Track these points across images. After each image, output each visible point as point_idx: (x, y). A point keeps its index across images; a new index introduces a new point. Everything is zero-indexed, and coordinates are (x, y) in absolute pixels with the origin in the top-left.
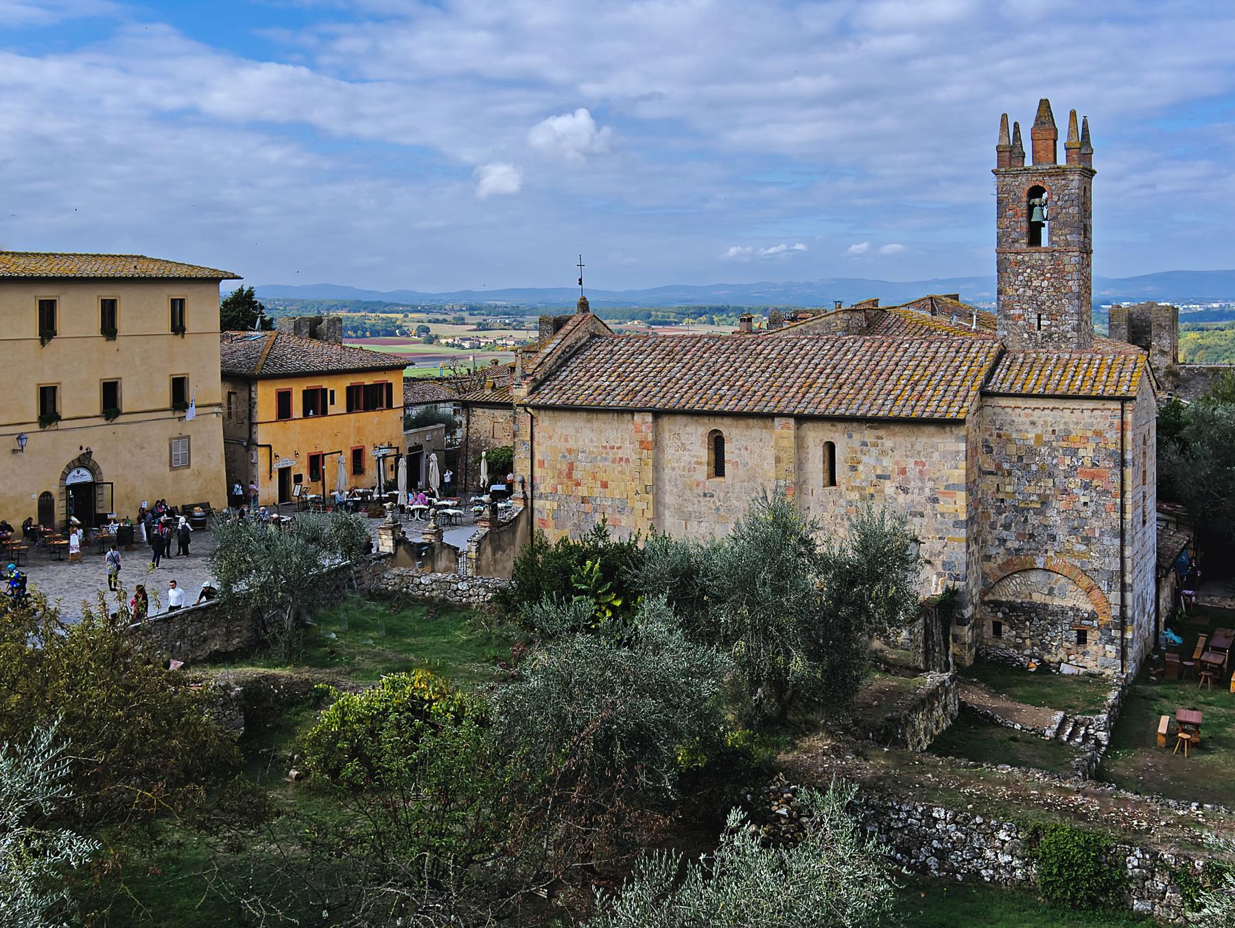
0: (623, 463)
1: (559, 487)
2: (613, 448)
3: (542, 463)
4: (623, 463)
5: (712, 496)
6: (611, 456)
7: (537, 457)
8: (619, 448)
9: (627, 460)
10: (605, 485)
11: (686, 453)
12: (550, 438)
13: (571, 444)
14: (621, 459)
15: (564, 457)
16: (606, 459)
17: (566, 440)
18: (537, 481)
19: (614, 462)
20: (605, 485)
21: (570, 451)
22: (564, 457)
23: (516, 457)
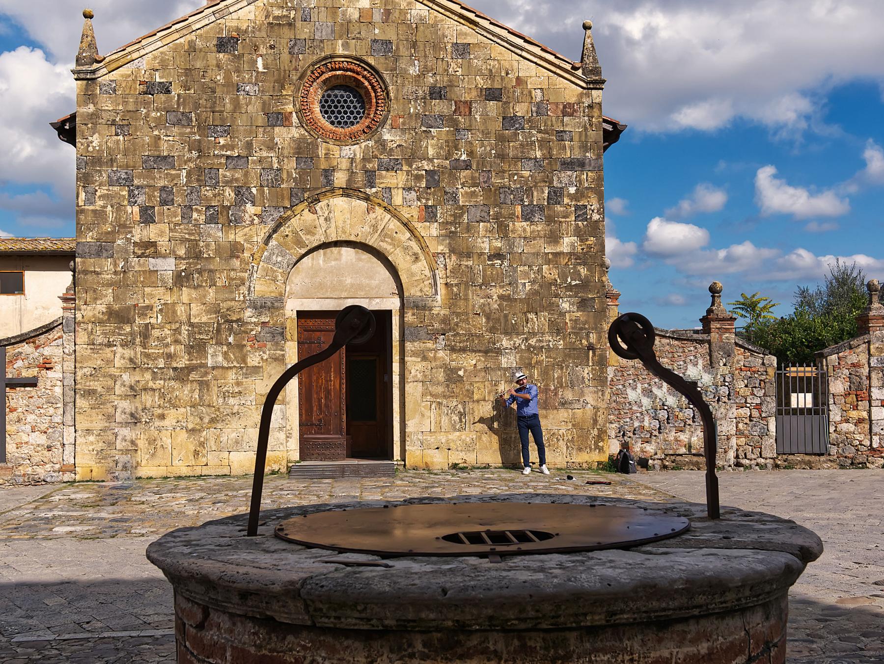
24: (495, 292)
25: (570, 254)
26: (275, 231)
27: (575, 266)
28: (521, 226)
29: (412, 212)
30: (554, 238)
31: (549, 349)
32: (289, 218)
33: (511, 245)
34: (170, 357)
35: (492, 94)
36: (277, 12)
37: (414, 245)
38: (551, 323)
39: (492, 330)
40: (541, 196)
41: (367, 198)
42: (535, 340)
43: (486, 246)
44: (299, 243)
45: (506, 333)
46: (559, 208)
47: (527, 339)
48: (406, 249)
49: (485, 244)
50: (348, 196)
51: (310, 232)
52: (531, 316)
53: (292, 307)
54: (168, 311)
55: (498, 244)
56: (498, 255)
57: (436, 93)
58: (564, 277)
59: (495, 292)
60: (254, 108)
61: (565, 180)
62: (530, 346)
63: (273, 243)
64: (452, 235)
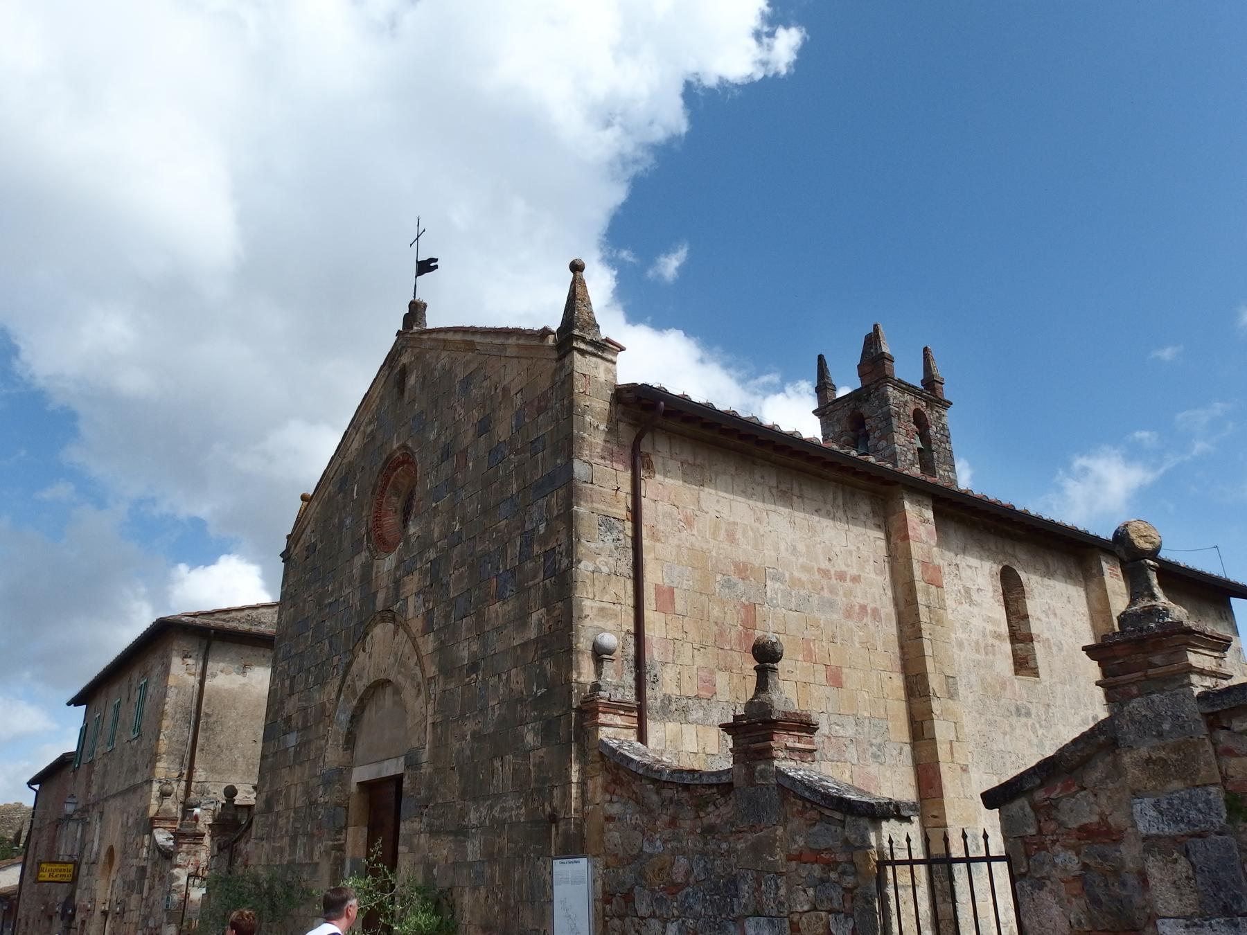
0: (868, 620)
1: (721, 679)
2: (841, 576)
3: (666, 596)
4: (868, 620)
5: (1028, 714)
6: (841, 600)
7: (652, 576)
8: (856, 579)
9: (875, 612)
10: (835, 679)
11: (975, 610)
12: (689, 522)
13: (744, 550)
14: (863, 608)
15: (728, 585)
16: (831, 604)
17: (731, 537)
18: (654, 653)
19: (848, 614)
20: (835, 679)
21: (743, 570)
22: (728, 585)
23: (585, 567)
24: (470, 727)
25: (537, 640)
26: (343, 682)
27: (541, 659)
28: (497, 611)
29: (417, 625)
30: (521, 619)
31: (512, 825)
32: (349, 665)
33: (484, 646)
34: (282, 850)
35: (484, 427)
36: (369, 429)
37: (417, 670)
38: (515, 772)
39: (463, 795)
40: (513, 551)
41: (394, 620)
42: (497, 808)
43: (465, 654)
44: (354, 693)
45: (474, 799)
46: (529, 565)
47: (491, 808)
48: (413, 678)
49: (465, 652)
50: (383, 620)
51: (361, 678)
52: (497, 764)
53: (362, 774)
54: (287, 796)
55: (475, 647)
56: (474, 667)
57: (446, 455)
58: (528, 683)
59: (470, 727)
60: (347, 544)
61: (536, 517)
62: (493, 819)
63: (342, 698)
64: (442, 648)
